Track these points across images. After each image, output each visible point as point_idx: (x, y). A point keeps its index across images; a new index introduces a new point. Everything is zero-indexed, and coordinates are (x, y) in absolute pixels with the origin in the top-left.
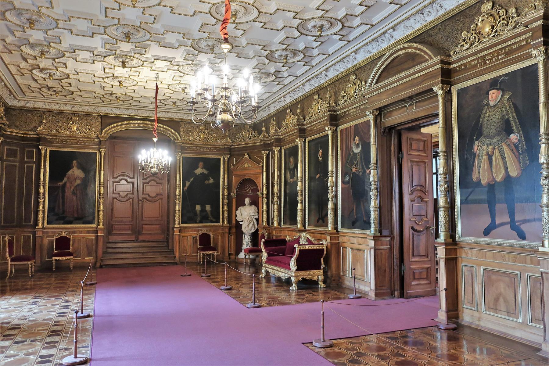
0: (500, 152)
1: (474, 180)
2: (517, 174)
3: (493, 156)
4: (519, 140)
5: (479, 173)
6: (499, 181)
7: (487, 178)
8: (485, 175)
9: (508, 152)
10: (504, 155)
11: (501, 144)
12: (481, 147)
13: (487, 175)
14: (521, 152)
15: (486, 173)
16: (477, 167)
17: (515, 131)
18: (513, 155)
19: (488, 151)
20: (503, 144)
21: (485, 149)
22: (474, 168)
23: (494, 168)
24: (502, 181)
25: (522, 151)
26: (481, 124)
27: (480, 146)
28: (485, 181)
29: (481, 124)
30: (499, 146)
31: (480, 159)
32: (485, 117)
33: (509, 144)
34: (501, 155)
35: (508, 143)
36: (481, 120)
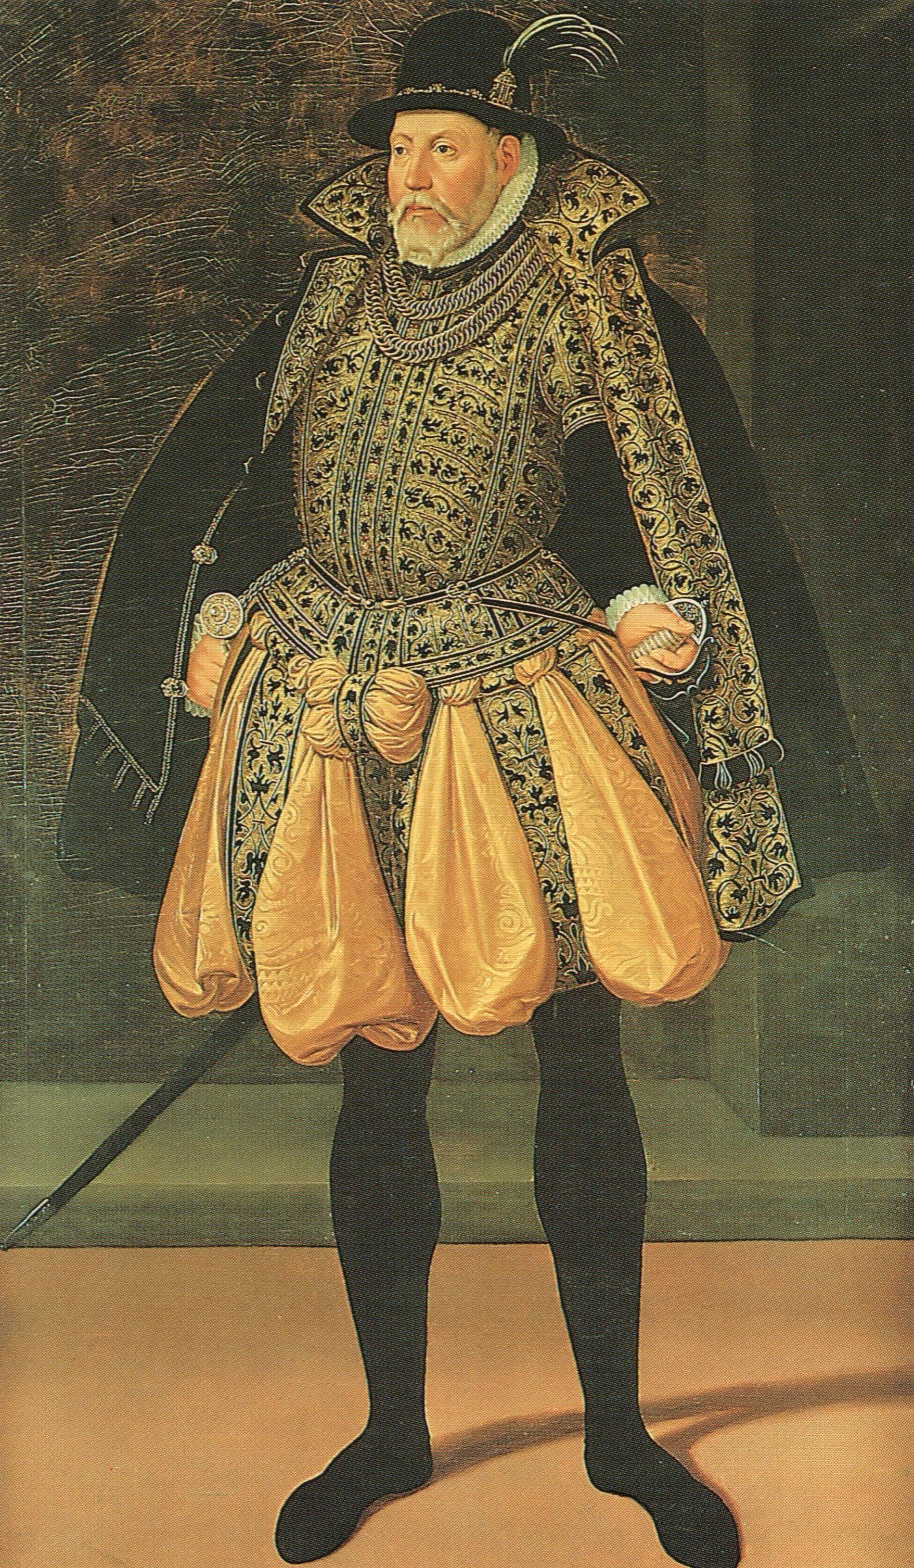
0: (496, 743)
1: (175, 999)
2: (670, 967)
3: (411, 770)
4: (708, 653)
5: (244, 927)
6: (484, 1024)
7: (335, 990)
8: (318, 954)
9: (589, 752)
10: (547, 772)
11: (511, 663)
12: (276, 660)
13: (339, 950)
14: (723, 773)
15: (332, 934)
16: (214, 867)
17: (672, 567)
18: (638, 784)
19: (363, 718)
20: (531, 665)
21: (321, 691)
22: (181, 871)
23: (423, 895)
24: (509, 1032)
25: (737, 767)
26: (290, 425)
27: (257, 656)
28: (316, 1020)
29: (290, 425)
30: (490, 680)
31: (260, 787)
32: (331, 367)
33: (601, 683)
34: (511, 778)
35: (584, 668)
36: (283, 389)
